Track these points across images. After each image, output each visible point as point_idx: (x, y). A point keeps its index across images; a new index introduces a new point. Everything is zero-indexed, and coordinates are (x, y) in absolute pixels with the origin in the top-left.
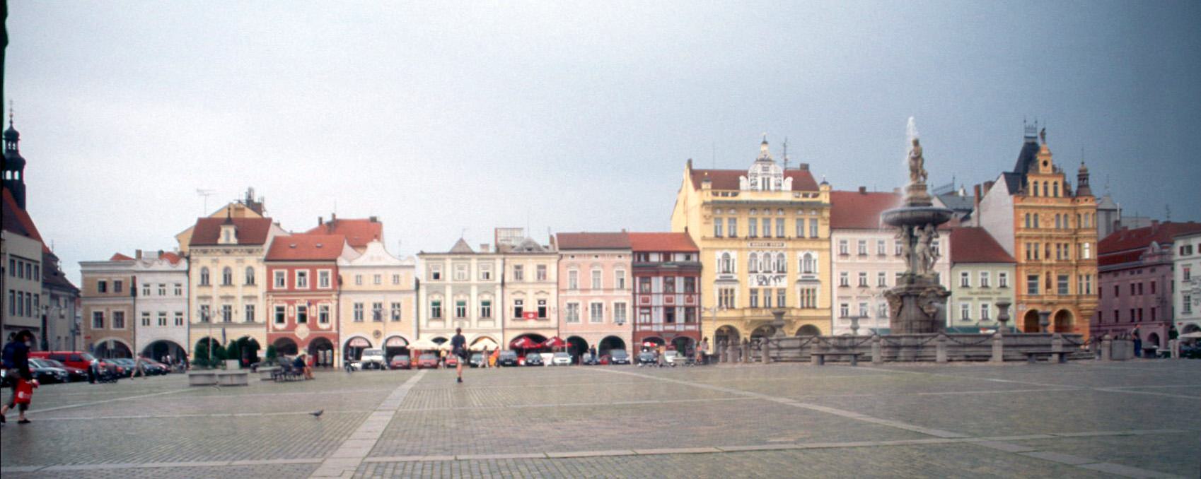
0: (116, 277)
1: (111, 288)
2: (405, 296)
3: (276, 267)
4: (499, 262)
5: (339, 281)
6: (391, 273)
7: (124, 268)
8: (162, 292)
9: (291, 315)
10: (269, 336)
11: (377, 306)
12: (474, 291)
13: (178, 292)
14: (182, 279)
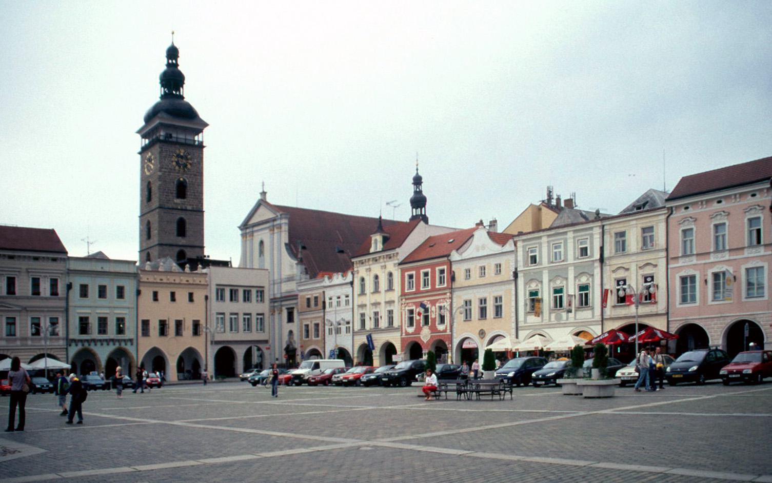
0: (316, 293)
1: (312, 302)
2: (504, 287)
3: (408, 270)
4: (597, 231)
5: (453, 279)
6: (493, 262)
7: (318, 285)
8: (339, 304)
9: (433, 316)
10: (403, 340)
11: (483, 301)
12: (571, 274)
13: (347, 302)
14: (348, 290)
